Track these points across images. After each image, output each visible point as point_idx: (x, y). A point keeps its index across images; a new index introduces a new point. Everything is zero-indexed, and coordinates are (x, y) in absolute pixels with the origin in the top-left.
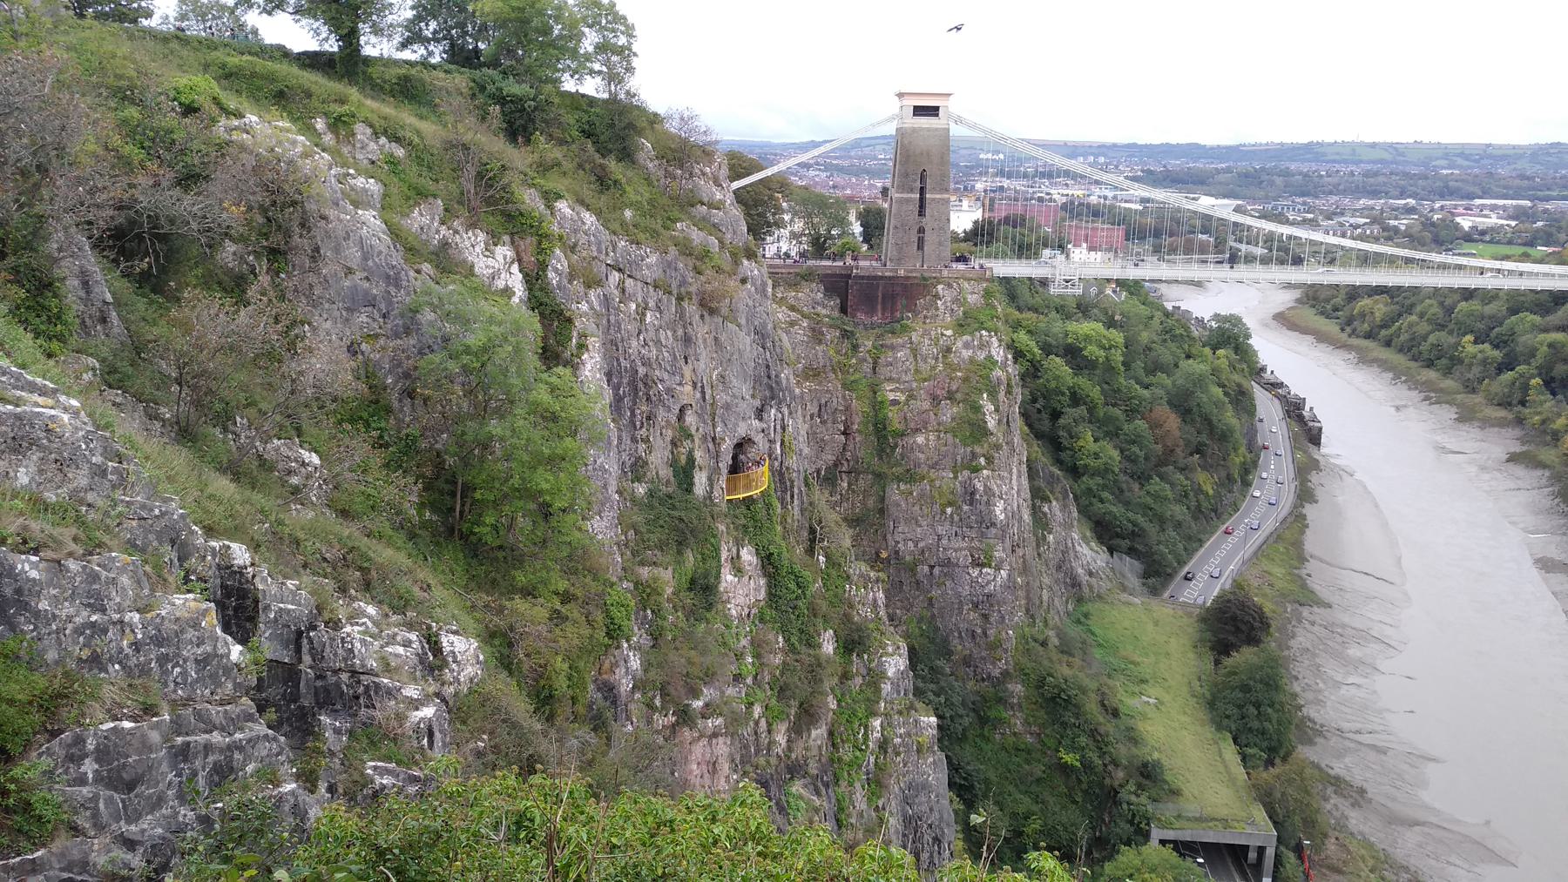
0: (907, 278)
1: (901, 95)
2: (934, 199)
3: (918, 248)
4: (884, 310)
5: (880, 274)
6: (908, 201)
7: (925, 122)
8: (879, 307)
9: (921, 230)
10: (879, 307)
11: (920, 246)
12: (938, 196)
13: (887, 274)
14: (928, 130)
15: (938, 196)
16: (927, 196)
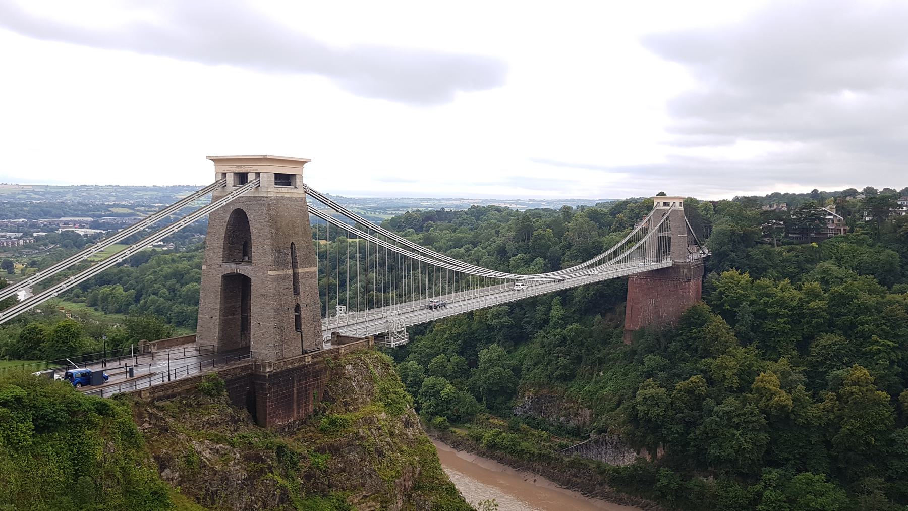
0: (314, 364)
1: (217, 161)
2: (304, 274)
3: (296, 329)
4: (299, 408)
5: (290, 366)
6: (284, 278)
7: (285, 191)
8: (295, 407)
9: (297, 308)
10: (295, 407)
11: (298, 327)
12: (307, 270)
13: (296, 365)
14: (290, 199)
15: (307, 270)
16: (300, 270)
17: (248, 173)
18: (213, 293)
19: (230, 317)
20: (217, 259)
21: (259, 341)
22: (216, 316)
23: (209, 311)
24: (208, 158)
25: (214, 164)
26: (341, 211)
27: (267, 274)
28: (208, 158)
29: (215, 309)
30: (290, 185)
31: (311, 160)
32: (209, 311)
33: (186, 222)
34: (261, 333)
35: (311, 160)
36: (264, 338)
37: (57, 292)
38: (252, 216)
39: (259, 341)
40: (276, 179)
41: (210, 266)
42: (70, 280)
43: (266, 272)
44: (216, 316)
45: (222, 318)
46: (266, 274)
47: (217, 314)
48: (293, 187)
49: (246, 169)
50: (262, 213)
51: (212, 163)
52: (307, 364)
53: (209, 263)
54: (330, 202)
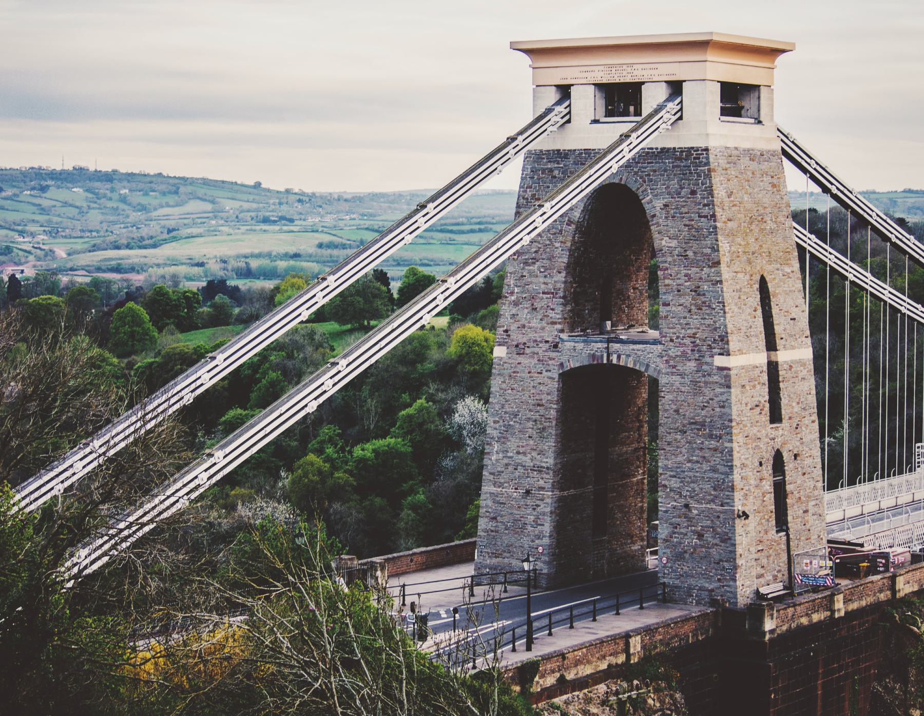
17: (643, 83)
18: (530, 424)
19: (572, 492)
20: (543, 329)
21: (687, 556)
22: (542, 488)
23: (517, 474)
24: (514, 46)
25: (531, 63)
26: (835, 191)
27: (711, 364)
28: (514, 46)
29: (539, 470)
30: (740, 116)
31: (793, 44)
32: (517, 474)
33: (545, 217)
34: (695, 532)
35: (793, 44)
36: (702, 546)
37: (315, 399)
38: (659, 204)
39: (687, 556)
40: (723, 99)
41: (520, 349)
42: (339, 367)
43: (708, 359)
44: (542, 488)
45: (557, 492)
46: (707, 364)
47: (546, 481)
48: (752, 121)
49: (635, 73)
50: (693, 193)
51: (526, 59)
52: (837, 616)
53: (517, 337)
54: (815, 166)
